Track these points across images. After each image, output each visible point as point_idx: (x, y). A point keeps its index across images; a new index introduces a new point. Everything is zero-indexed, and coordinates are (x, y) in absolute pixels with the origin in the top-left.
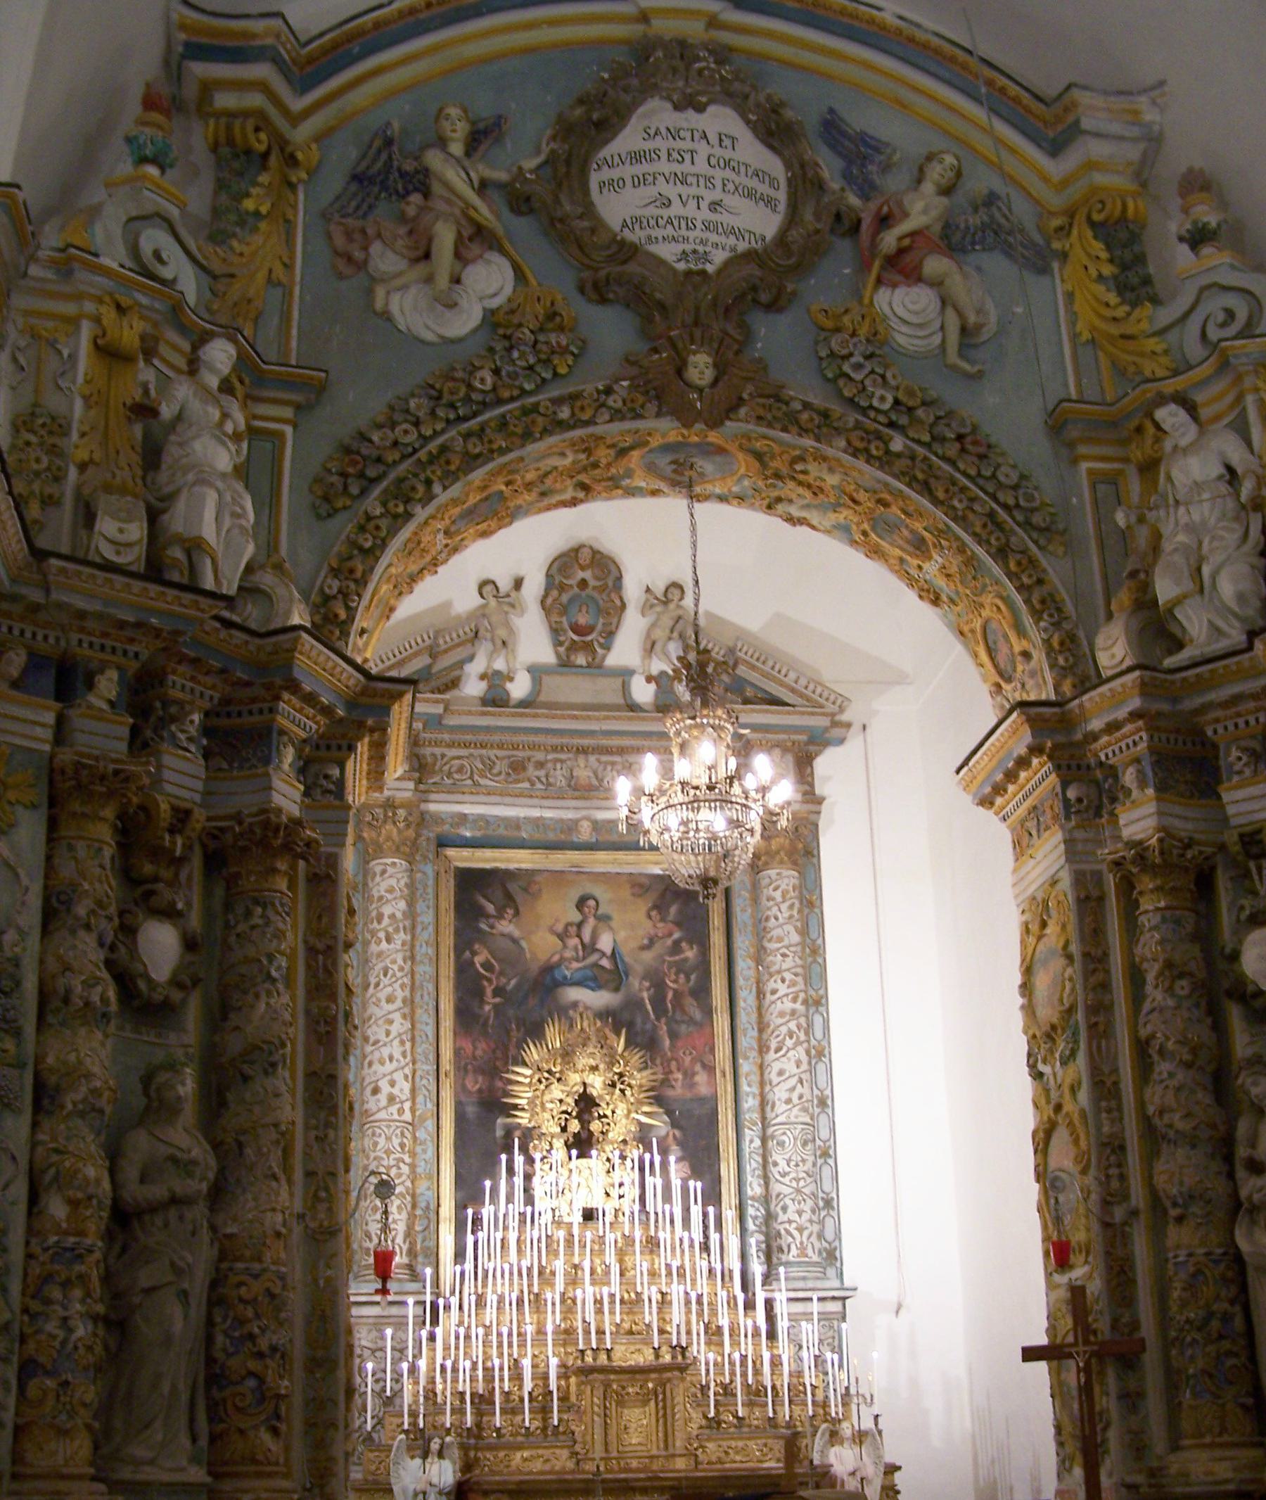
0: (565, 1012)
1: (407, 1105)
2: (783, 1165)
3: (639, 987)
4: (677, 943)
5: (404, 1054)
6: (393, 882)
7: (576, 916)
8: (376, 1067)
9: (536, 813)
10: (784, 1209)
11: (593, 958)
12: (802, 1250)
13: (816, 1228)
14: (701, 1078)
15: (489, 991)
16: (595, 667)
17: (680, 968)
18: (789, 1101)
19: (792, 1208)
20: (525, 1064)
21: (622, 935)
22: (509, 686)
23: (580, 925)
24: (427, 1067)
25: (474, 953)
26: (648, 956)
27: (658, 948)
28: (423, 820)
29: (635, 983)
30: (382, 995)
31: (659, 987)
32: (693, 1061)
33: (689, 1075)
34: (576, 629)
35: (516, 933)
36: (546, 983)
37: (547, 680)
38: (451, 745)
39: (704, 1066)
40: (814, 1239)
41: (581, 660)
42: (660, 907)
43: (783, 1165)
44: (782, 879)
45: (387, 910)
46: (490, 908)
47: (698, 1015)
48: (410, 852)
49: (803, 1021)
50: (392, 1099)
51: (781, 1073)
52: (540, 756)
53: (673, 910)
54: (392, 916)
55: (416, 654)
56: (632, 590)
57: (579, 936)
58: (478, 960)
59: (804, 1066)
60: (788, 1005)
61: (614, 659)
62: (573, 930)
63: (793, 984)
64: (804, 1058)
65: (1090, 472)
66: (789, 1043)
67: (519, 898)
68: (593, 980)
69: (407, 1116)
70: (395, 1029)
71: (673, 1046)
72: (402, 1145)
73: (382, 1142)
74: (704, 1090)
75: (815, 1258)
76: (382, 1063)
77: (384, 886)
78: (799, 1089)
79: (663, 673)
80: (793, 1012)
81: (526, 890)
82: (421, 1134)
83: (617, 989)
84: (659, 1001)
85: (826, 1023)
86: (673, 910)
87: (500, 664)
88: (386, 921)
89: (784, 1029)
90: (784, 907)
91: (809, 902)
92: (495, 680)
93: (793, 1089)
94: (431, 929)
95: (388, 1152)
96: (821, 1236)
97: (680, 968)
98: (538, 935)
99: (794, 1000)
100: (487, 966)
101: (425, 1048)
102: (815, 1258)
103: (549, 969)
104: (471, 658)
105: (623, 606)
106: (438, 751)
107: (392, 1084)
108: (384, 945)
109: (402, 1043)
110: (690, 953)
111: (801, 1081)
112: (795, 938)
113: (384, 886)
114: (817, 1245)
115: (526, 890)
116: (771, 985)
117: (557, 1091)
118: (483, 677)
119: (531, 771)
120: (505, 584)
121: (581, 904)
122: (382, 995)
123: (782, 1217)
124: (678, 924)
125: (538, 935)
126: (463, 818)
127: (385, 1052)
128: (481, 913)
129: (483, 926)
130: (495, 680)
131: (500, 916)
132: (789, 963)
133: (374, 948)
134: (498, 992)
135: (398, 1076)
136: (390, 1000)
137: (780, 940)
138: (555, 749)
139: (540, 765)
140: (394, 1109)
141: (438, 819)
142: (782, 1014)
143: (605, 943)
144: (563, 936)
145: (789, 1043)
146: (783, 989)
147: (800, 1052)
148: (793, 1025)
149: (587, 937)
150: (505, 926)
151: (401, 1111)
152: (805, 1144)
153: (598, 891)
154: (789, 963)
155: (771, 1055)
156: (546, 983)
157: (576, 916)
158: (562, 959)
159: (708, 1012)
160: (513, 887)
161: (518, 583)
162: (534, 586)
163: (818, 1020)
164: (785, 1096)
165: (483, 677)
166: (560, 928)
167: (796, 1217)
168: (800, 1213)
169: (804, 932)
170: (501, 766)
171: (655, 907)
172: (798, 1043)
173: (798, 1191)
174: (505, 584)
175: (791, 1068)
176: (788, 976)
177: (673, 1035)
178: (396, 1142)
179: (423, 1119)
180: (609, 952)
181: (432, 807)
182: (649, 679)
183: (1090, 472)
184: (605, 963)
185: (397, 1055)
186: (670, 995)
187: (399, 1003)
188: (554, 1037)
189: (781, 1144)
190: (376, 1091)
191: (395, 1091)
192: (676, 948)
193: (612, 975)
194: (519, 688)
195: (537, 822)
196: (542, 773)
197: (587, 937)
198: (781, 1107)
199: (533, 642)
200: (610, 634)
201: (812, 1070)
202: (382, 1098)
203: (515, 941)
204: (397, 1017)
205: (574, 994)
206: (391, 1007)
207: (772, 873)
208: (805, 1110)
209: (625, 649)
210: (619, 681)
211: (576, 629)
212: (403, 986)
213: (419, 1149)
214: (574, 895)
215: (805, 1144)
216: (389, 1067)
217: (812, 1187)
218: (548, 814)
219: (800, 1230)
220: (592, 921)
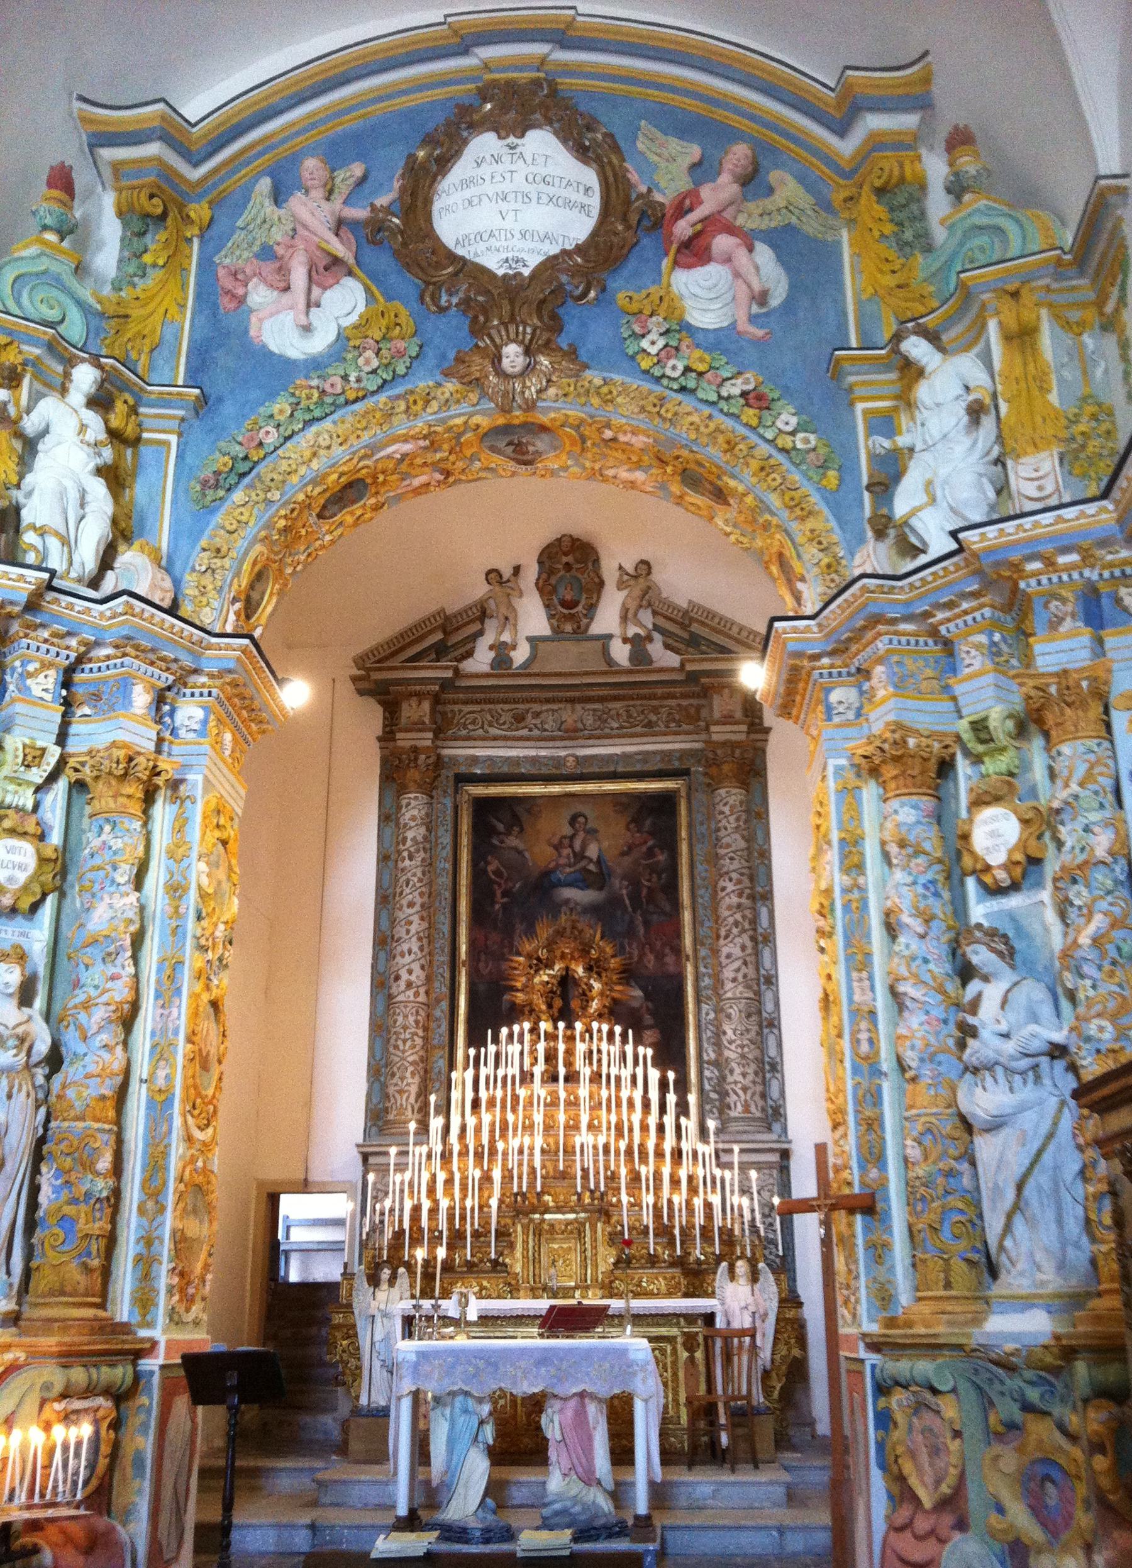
0: (555, 909)
1: (422, 990)
2: (730, 1033)
3: (619, 886)
4: (650, 849)
5: (421, 949)
6: (415, 812)
7: (567, 830)
8: (398, 959)
9: (532, 753)
10: (732, 1072)
11: (583, 863)
12: (747, 1109)
13: (759, 1088)
14: (670, 959)
15: (499, 893)
16: (580, 633)
17: (653, 869)
18: (734, 980)
19: (738, 1071)
20: (519, 954)
21: (606, 844)
22: (512, 654)
23: (572, 838)
24: (444, 958)
25: (487, 863)
26: (627, 861)
27: (635, 854)
28: (439, 763)
29: (616, 883)
30: (404, 902)
31: (634, 883)
32: (664, 945)
33: (660, 957)
34: (565, 604)
35: (522, 847)
36: (543, 887)
37: (541, 646)
38: (466, 702)
39: (672, 949)
40: (757, 1098)
41: (568, 628)
42: (636, 821)
43: (730, 1033)
44: (730, 797)
45: (410, 834)
46: (501, 827)
47: (668, 908)
48: (429, 789)
49: (748, 913)
50: (409, 985)
51: (728, 956)
52: (536, 707)
53: (648, 822)
54: (414, 839)
55: (431, 632)
56: (609, 571)
57: (571, 846)
58: (490, 868)
59: (749, 951)
60: (735, 900)
61: (596, 629)
62: (566, 842)
63: (739, 882)
64: (749, 944)
65: (866, 412)
66: (735, 931)
67: (524, 818)
68: (584, 880)
69: (422, 998)
70: (413, 929)
71: (647, 931)
72: (417, 1022)
73: (400, 1019)
74: (672, 969)
75: (758, 1114)
76: (402, 955)
77: (408, 816)
78: (744, 970)
79: (637, 635)
80: (739, 906)
81: (529, 811)
82: (437, 1013)
83: (601, 889)
84: (635, 897)
85: (771, 913)
86: (648, 822)
87: (506, 637)
88: (409, 843)
89: (731, 920)
90: (732, 819)
91: (756, 816)
92: (502, 651)
93: (738, 970)
94: (449, 848)
95: (405, 1028)
96: (764, 1096)
97: (653, 869)
98: (538, 848)
99: (740, 895)
100: (497, 873)
101: (444, 943)
102: (758, 1114)
103: (547, 873)
104: (481, 633)
105: (601, 584)
106: (456, 708)
107: (410, 972)
108: (407, 862)
109: (420, 939)
110: (661, 857)
111: (745, 963)
112: (742, 844)
113: (408, 816)
114: (761, 1103)
115: (529, 811)
116: (722, 883)
117: (544, 977)
118: (491, 648)
119: (530, 720)
120: (507, 573)
121: (573, 821)
122: (404, 902)
123: (730, 1079)
124: (652, 834)
125: (538, 848)
126: (475, 760)
127: (405, 947)
128: (493, 831)
129: (495, 842)
130: (502, 651)
131: (508, 833)
132: (736, 865)
133: (401, 865)
134: (505, 894)
135: (416, 967)
136: (411, 905)
137: (728, 846)
138: (548, 701)
139: (537, 715)
140: (411, 993)
141: (454, 760)
142: (729, 908)
143: (592, 851)
144: (557, 847)
145: (735, 931)
146: (730, 887)
147: (746, 939)
148: (738, 916)
149: (577, 847)
150: (513, 841)
151: (417, 994)
152: (749, 1016)
153: (587, 810)
154: (736, 865)
155: (722, 942)
156: (543, 887)
157: (567, 830)
158: (558, 866)
159: (676, 905)
160: (520, 810)
161: (517, 570)
162: (531, 572)
163: (764, 912)
164: (732, 975)
165: (491, 648)
166: (556, 841)
167: (740, 1078)
168: (744, 1075)
169: (749, 839)
170: (506, 717)
171: (633, 820)
172: (744, 931)
173: (743, 1056)
174: (507, 573)
175: (737, 952)
176: (734, 875)
177: (647, 923)
178: (411, 1019)
179: (438, 1001)
180: (595, 857)
181: (446, 752)
182: (625, 640)
183: (866, 412)
184: (592, 867)
185: (415, 949)
186: (645, 892)
187: (417, 908)
188: (544, 932)
189: (729, 1016)
190: (398, 978)
191: (413, 978)
192: (650, 853)
193: (597, 878)
194: (520, 655)
195: (534, 760)
196: (537, 721)
197: (577, 847)
198: (729, 985)
199: (533, 618)
200: (592, 608)
201: (757, 953)
202: (402, 984)
203: (520, 852)
204: (416, 919)
205: (568, 893)
206: (411, 911)
207: (722, 792)
208: (748, 987)
209: (607, 618)
210: (599, 644)
211: (565, 604)
212: (421, 894)
213: (433, 1025)
214: (567, 814)
215: (749, 1016)
216: (408, 959)
217: (757, 1053)
218: (543, 753)
219: (745, 1089)
220: (581, 834)
